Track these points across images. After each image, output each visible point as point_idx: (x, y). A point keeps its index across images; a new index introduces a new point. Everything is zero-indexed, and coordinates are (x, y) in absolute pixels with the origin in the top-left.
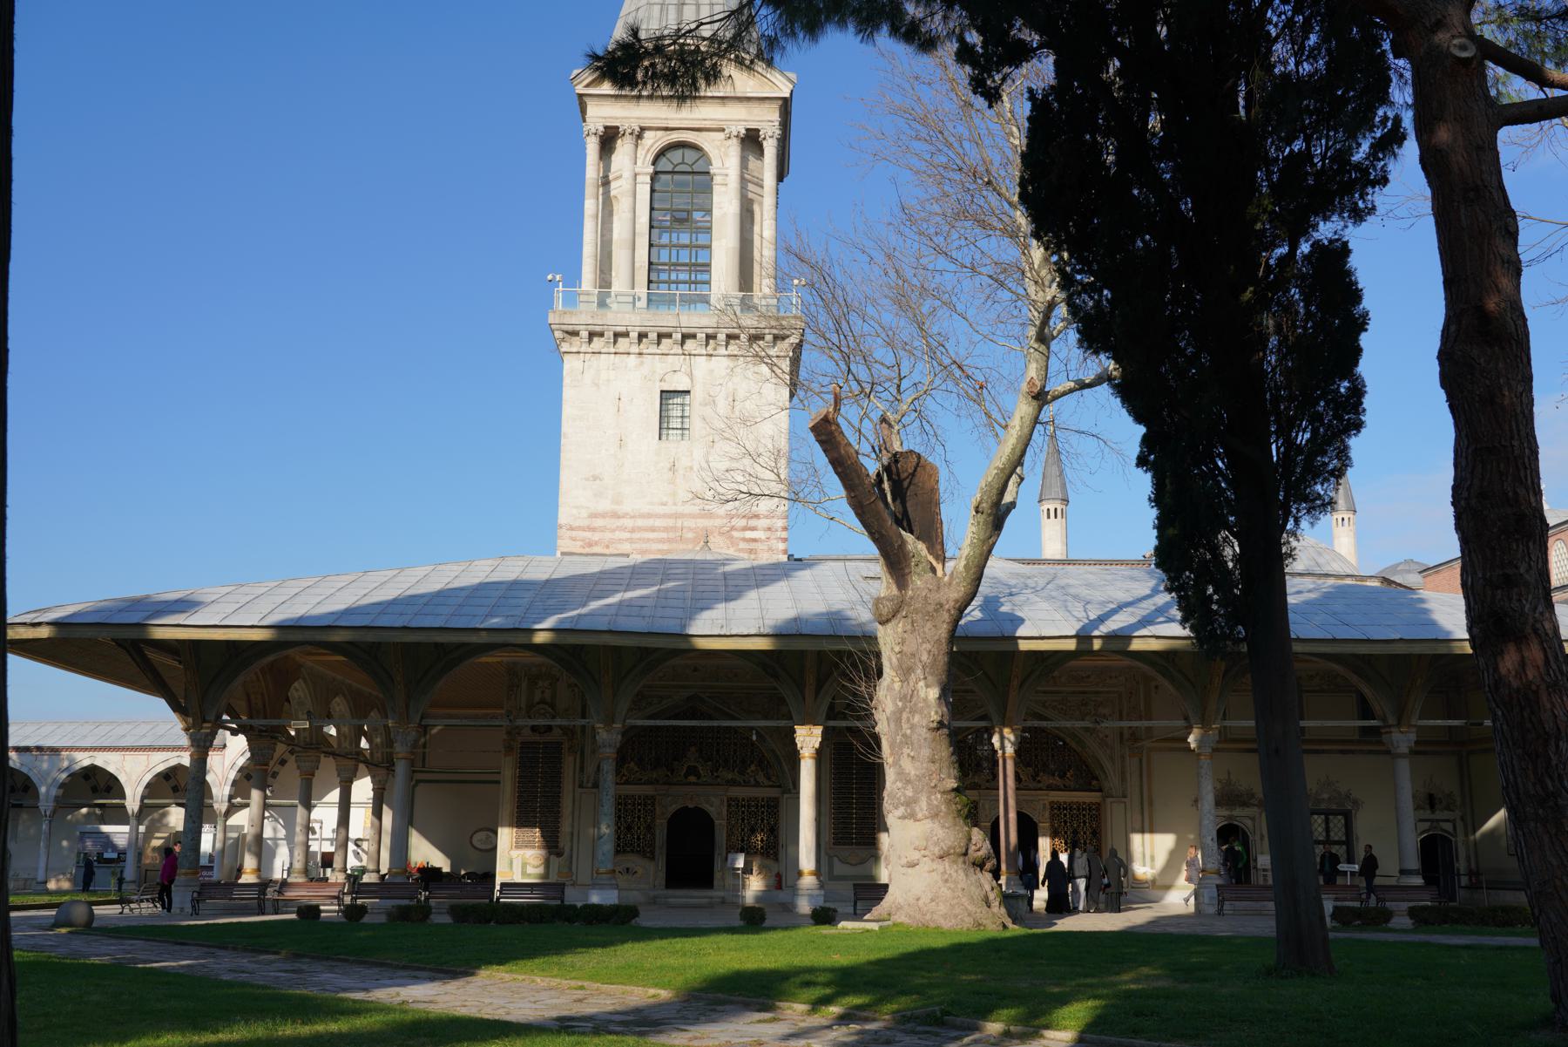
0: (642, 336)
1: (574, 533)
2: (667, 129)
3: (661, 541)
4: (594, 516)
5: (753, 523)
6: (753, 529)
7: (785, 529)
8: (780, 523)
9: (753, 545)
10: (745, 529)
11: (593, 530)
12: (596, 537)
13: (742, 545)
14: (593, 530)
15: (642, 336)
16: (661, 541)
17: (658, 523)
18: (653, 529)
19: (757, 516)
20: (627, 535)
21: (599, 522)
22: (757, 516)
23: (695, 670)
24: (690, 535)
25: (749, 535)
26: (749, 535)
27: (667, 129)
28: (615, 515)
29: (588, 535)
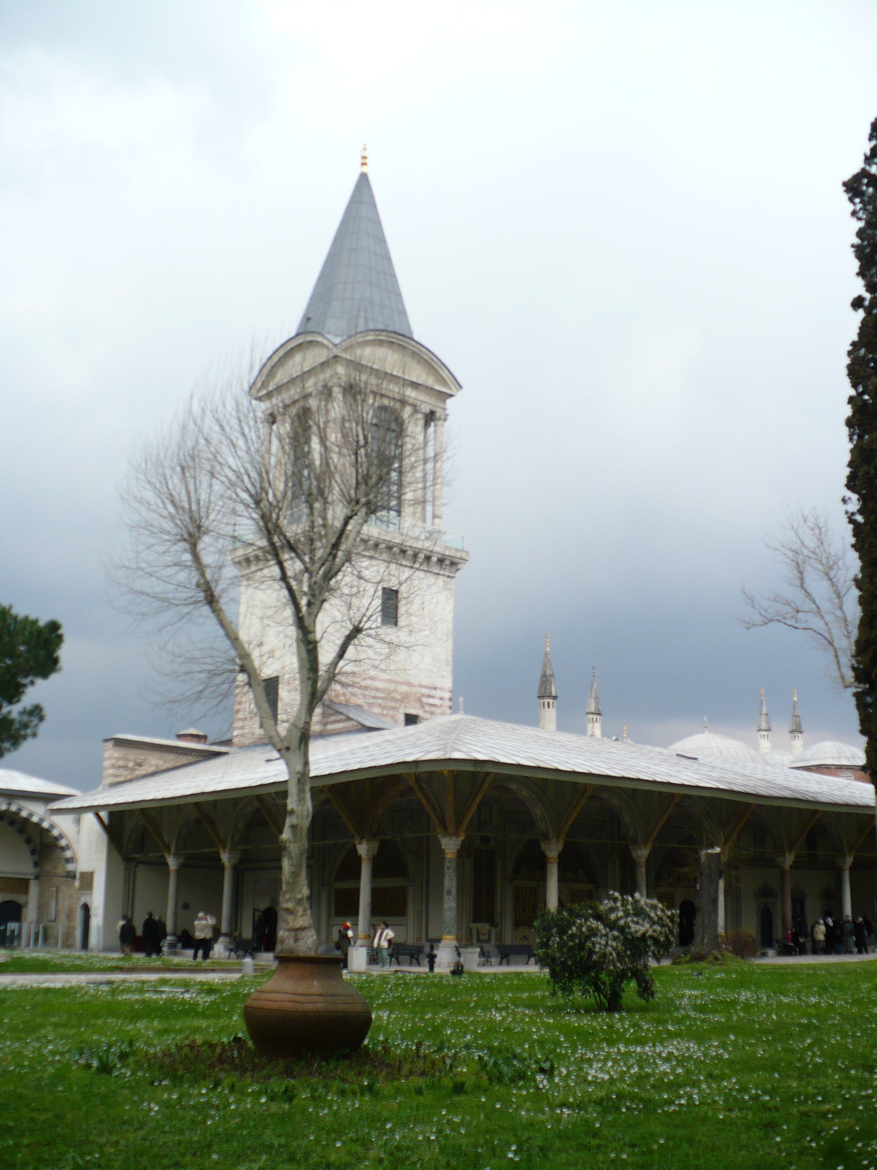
0: (376, 545)
3: (382, 698)
5: (433, 692)
6: (433, 697)
7: (450, 700)
8: (447, 695)
9: (433, 709)
10: (429, 696)
13: (427, 708)
16: (382, 698)
17: (379, 685)
18: (377, 689)
19: (435, 688)
22: (435, 688)
24: (399, 697)
25: (431, 701)
26: (431, 701)
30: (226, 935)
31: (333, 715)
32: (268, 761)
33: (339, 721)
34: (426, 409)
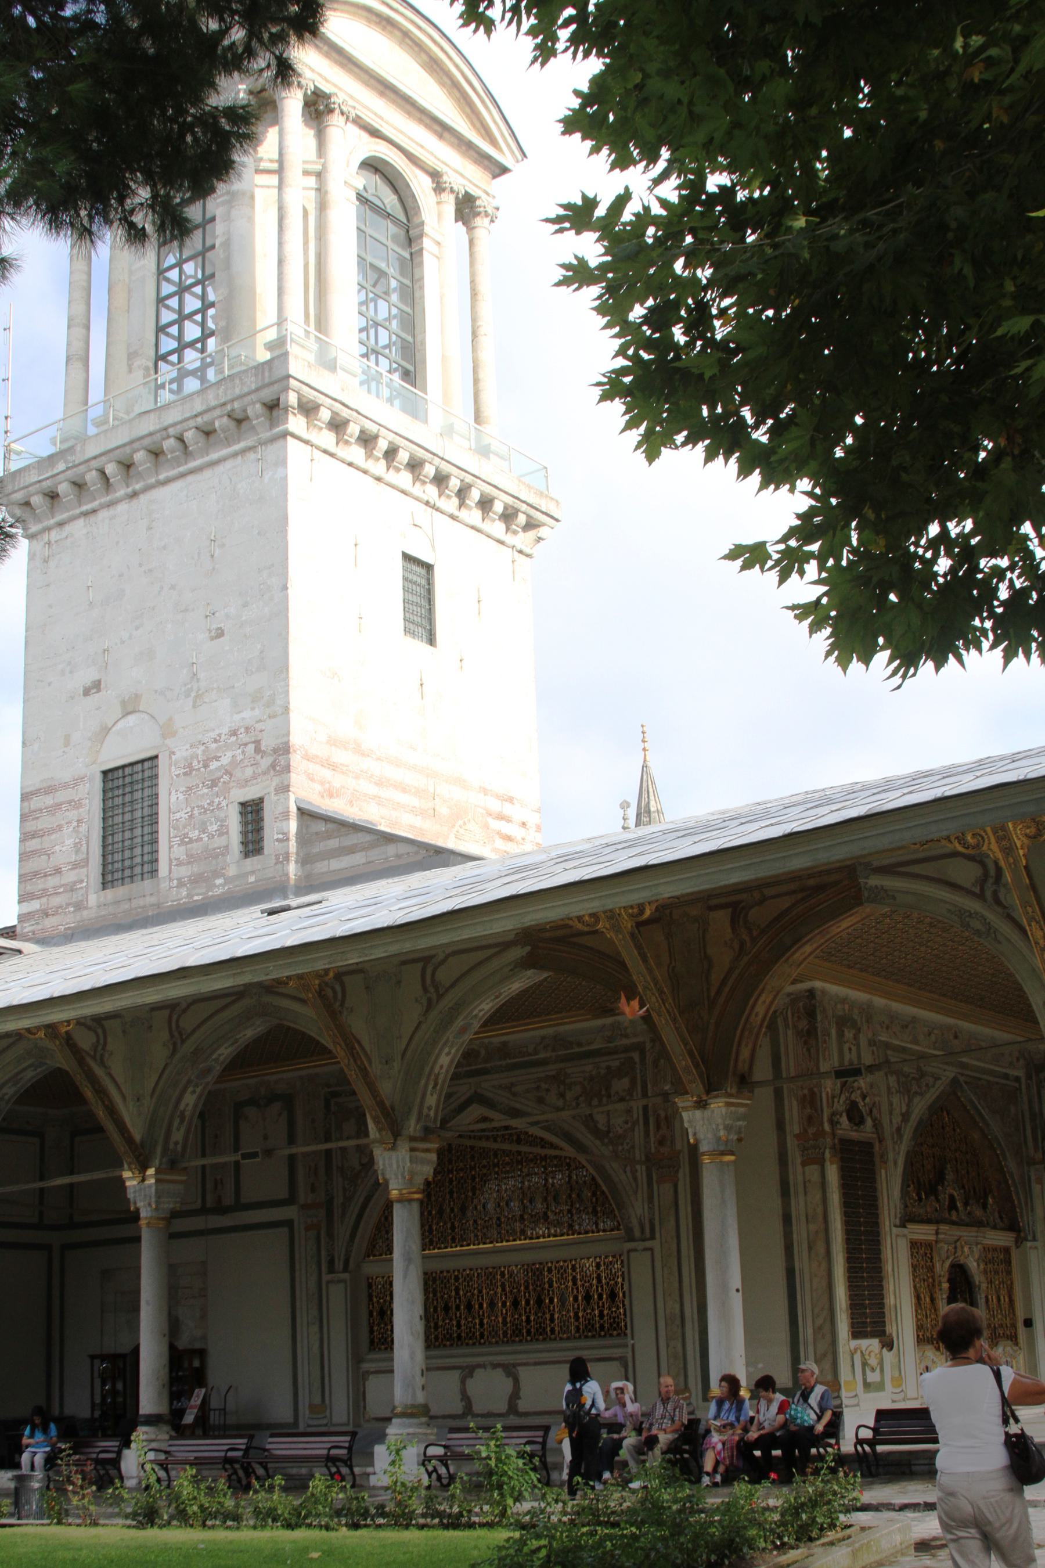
1: (312, 767)
2: (375, 133)
4: (333, 742)
5: (508, 809)
11: (333, 767)
12: (337, 781)
14: (333, 767)
15: (391, 454)
19: (511, 800)
20: (372, 789)
21: (340, 756)
22: (511, 800)
23: (956, 1037)
27: (375, 133)
28: (359, 751)
29: (326, 773)
30: (152, 1420)
31: (329, 836)
32: (272, 912)
33: (351, 850)
34: (460, 185)
